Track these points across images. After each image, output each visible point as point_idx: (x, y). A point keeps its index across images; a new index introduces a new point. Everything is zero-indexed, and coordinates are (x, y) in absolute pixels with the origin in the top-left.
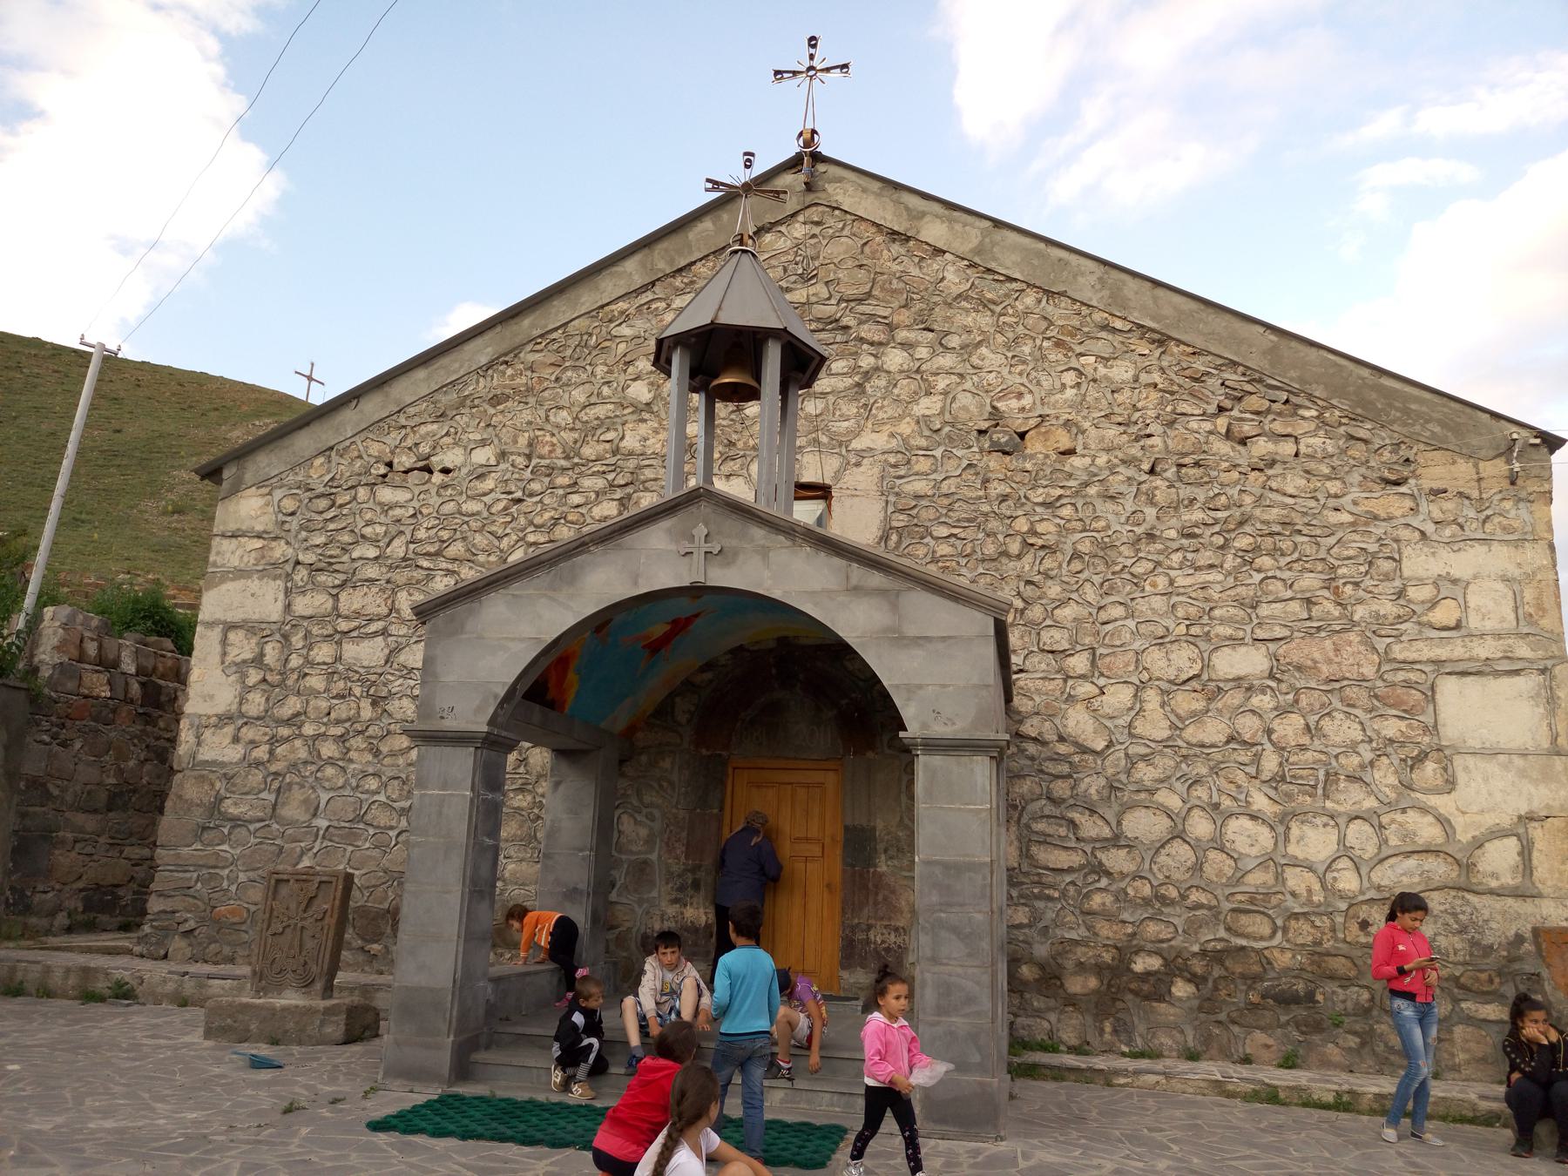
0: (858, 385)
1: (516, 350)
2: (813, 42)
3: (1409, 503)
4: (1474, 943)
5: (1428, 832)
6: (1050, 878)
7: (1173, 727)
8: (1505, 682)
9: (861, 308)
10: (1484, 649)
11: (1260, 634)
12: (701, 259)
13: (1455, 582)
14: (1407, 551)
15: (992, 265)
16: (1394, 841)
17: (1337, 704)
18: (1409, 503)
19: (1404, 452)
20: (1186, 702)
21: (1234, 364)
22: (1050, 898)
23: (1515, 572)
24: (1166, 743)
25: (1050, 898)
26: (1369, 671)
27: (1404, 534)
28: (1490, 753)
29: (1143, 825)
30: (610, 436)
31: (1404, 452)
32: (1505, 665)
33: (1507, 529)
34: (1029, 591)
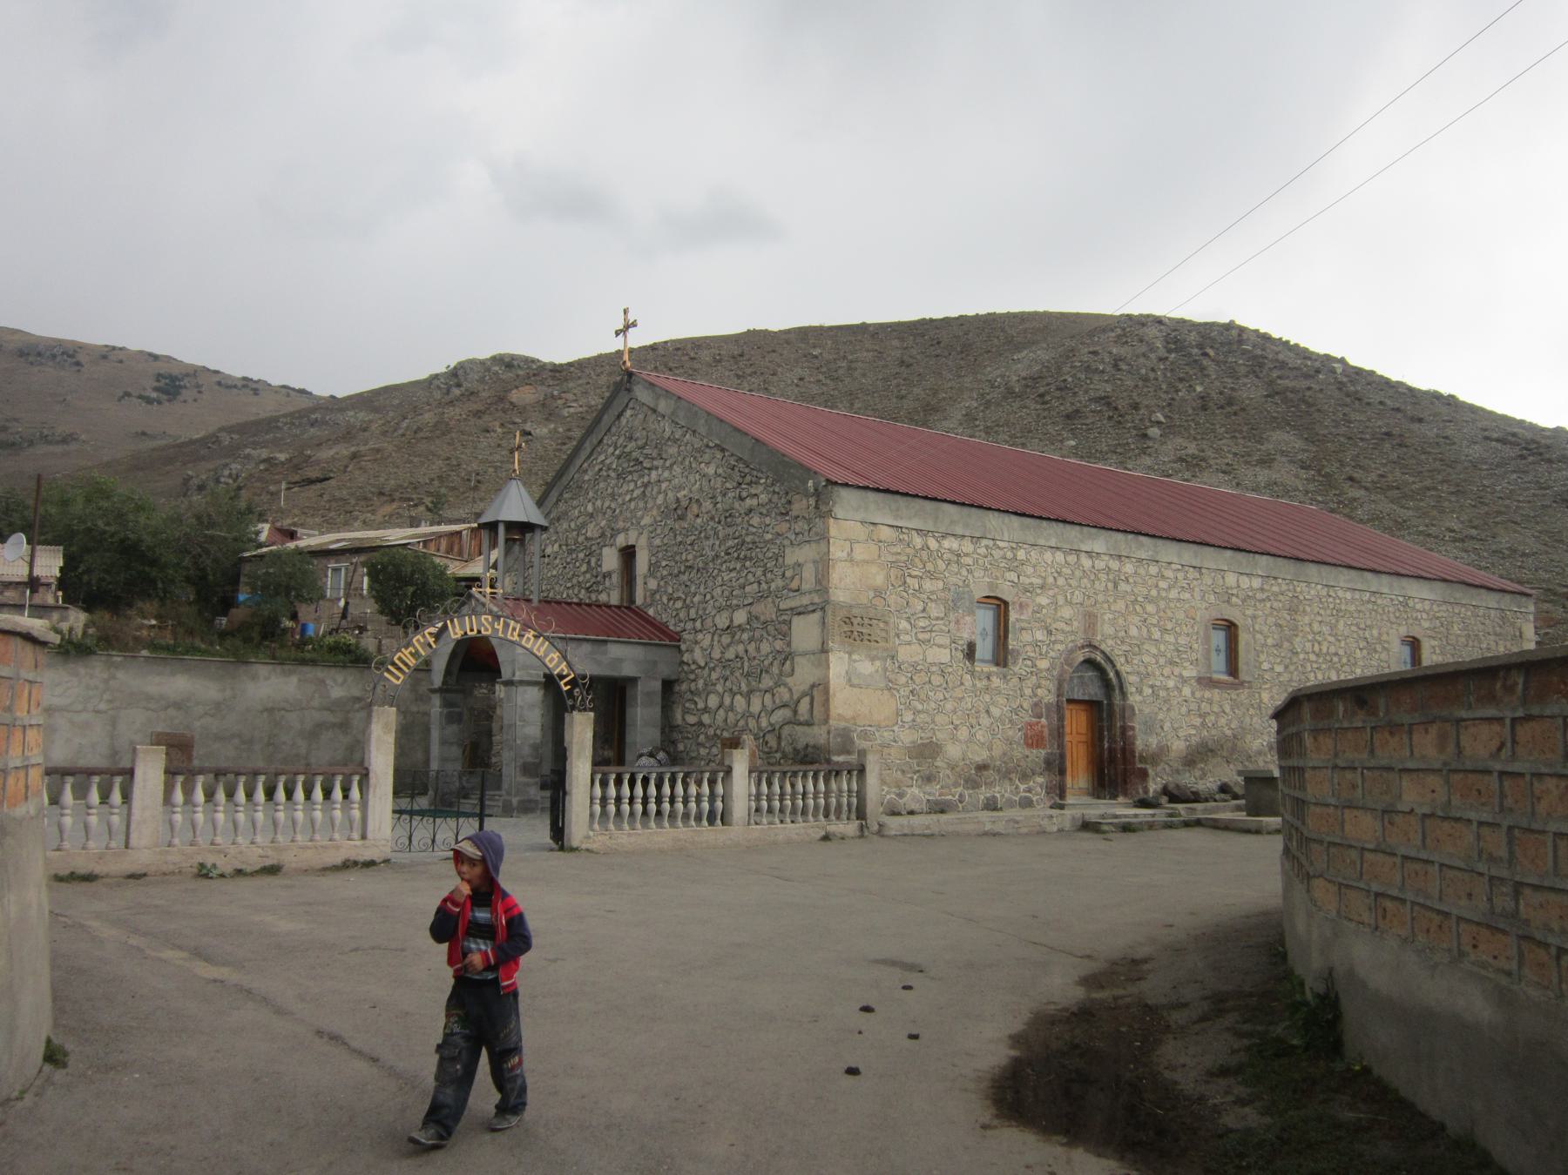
0: (644, 492)
1: (561, 495)
2: (625, 312)
3: (788, 525)
4: (795, 749)
5: (786, 696)
6: (690, 729)
7: (722, 653)
8: (811, 615)
9: (645, 451)
10: (805, 600)
11: (746, 603)
12: (605, 434)
13: (799, 565)
14: (787, 551)
15: (677, 420)
16: (777, 701)
17: (765, 635)
18: (788, 525)
19: (789, 497)
20: (726, 639)
21: (741, 459)
22: (688, 738)
23: (817, 557)
24: (719, 660)
25: (688, 738)
26: (774, 617)
27: (786, 542)
28: (804, 654)
29: (713, 701)
30: (584, 531)
31: (789, 497)
32: (811, 608)
33: (817, 534)
34: (687, 590)
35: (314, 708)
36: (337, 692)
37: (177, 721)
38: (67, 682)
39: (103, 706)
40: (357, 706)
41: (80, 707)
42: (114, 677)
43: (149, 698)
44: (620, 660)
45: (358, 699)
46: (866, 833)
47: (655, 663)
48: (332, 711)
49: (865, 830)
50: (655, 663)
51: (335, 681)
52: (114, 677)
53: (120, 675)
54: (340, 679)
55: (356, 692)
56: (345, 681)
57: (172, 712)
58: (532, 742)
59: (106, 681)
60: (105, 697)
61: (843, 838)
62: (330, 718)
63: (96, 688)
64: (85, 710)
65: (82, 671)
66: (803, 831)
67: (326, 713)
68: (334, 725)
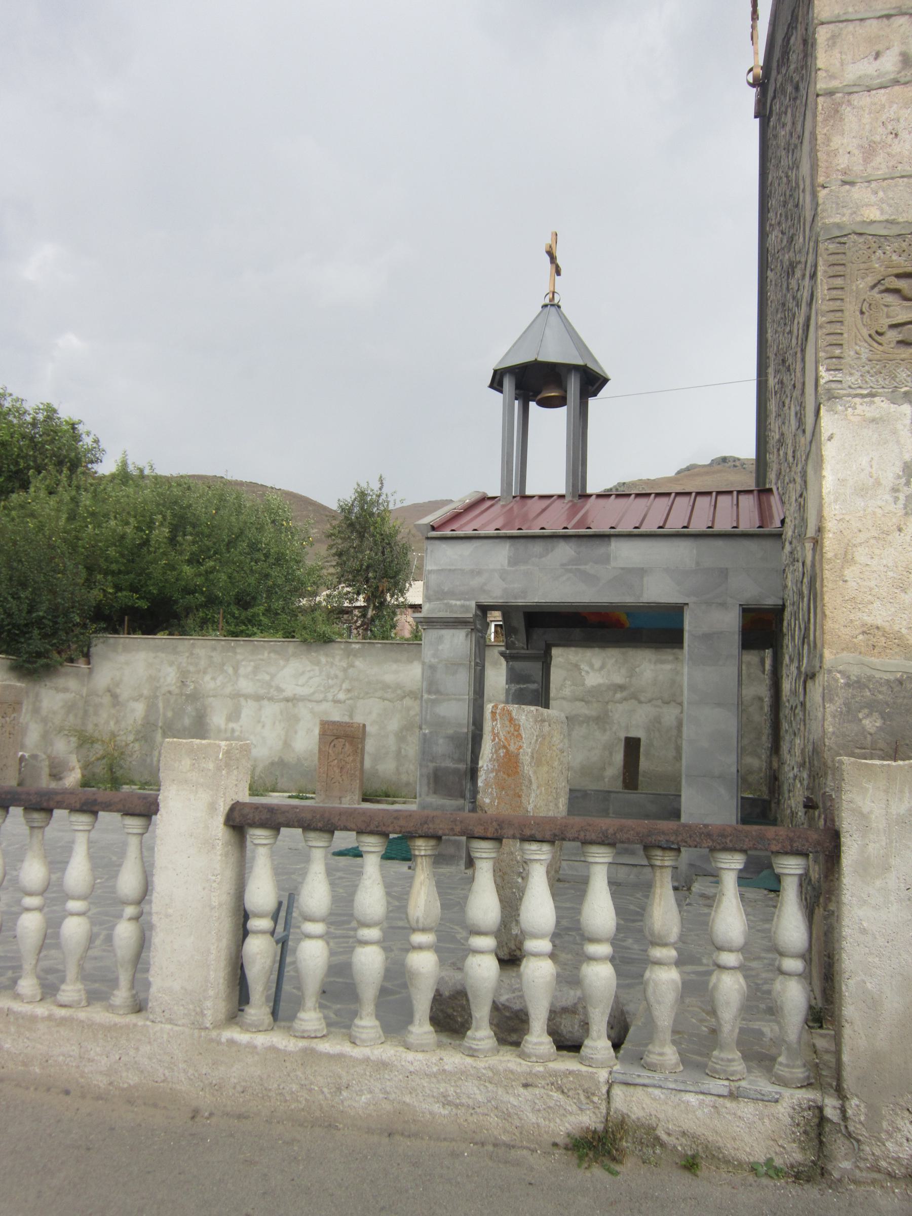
35: (564, 698)
36: (593, 679)
37: (412, 713)
38: (309, 671)
39: (341, 696)
40: (619, 696)
41: (321, 696)
42: (352, 666)
43: (386, 687)
44: (641, 572)
45: (622, 688)
46: (843, 1165)
47: (724, 573)
48: (587, 702)
49: (839, 1146)
50: (724, 573)
51: (592, 666)
52: (352, 666)
53: (358, 663)
54: (597, 664)
55: (618, 679)
56: (602, 667)
57: (408, 702)
58: (450, 731)
59: (345, 670)
60: (344, 686)
61: (690, 1165)
62: (582, 709)
63: (336, 677)
64: (325, 699)
65: (323, 660)
66: (474, 1091)
67: (578, 704)
68: (588, 719)
